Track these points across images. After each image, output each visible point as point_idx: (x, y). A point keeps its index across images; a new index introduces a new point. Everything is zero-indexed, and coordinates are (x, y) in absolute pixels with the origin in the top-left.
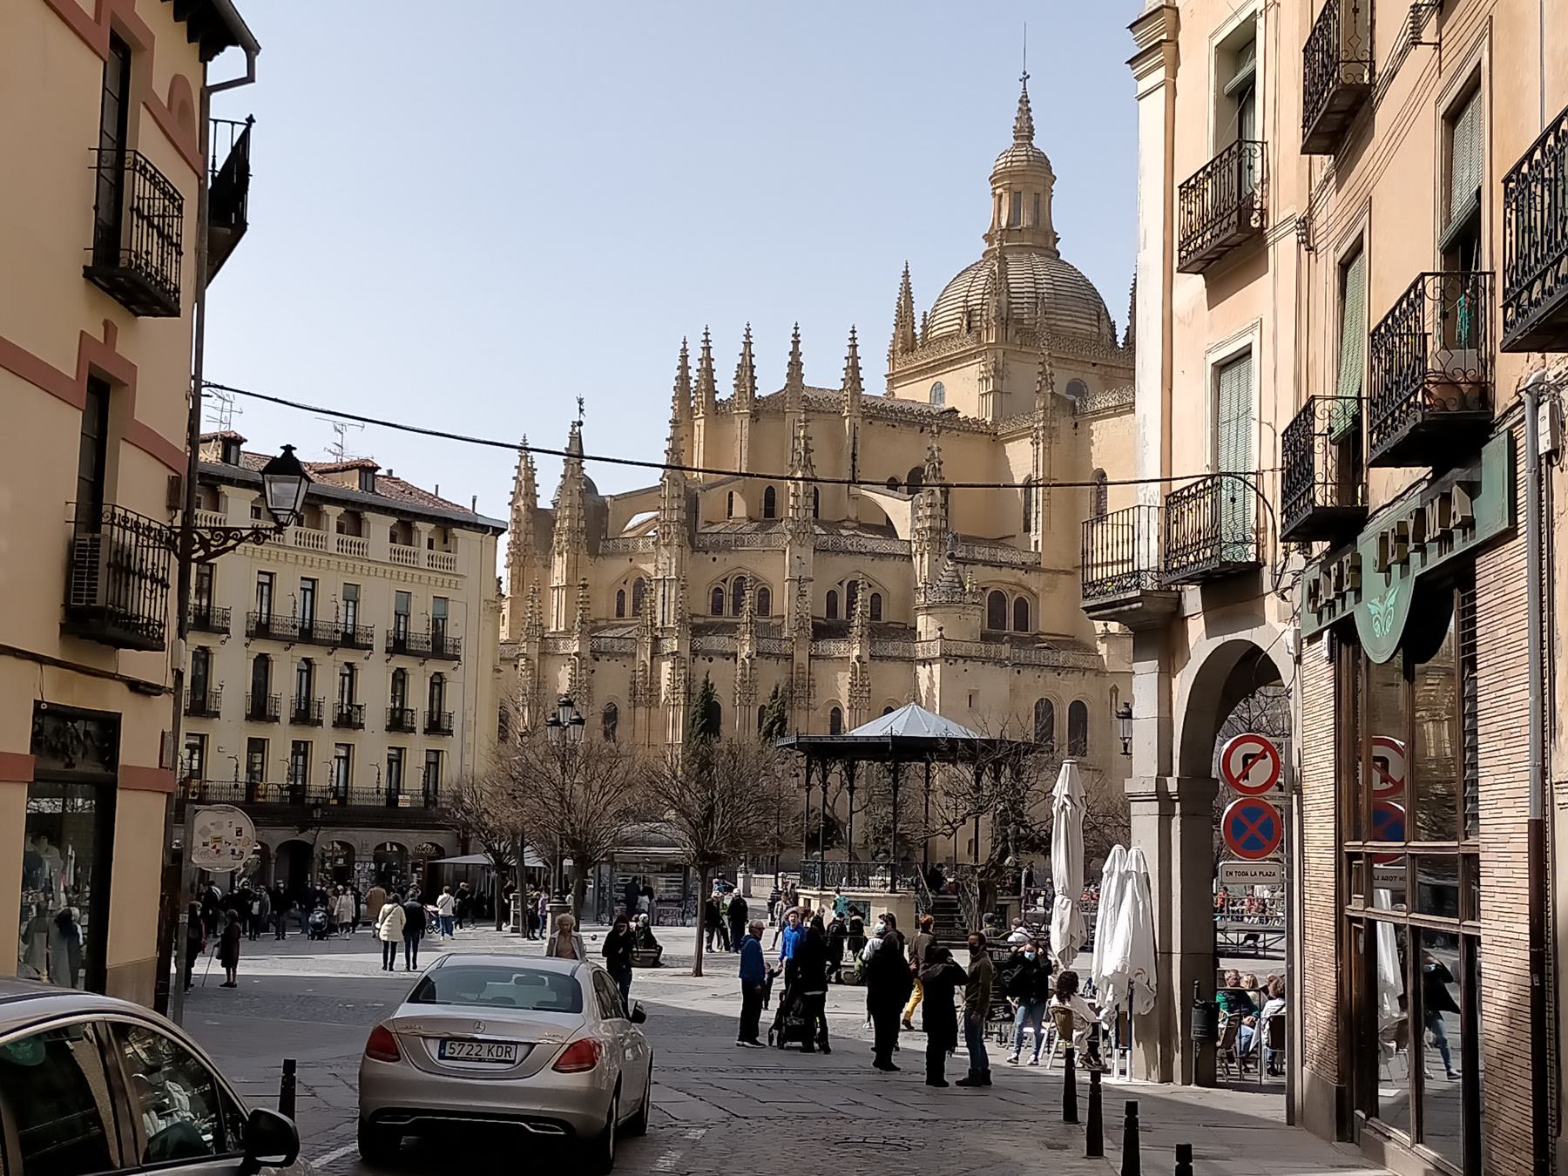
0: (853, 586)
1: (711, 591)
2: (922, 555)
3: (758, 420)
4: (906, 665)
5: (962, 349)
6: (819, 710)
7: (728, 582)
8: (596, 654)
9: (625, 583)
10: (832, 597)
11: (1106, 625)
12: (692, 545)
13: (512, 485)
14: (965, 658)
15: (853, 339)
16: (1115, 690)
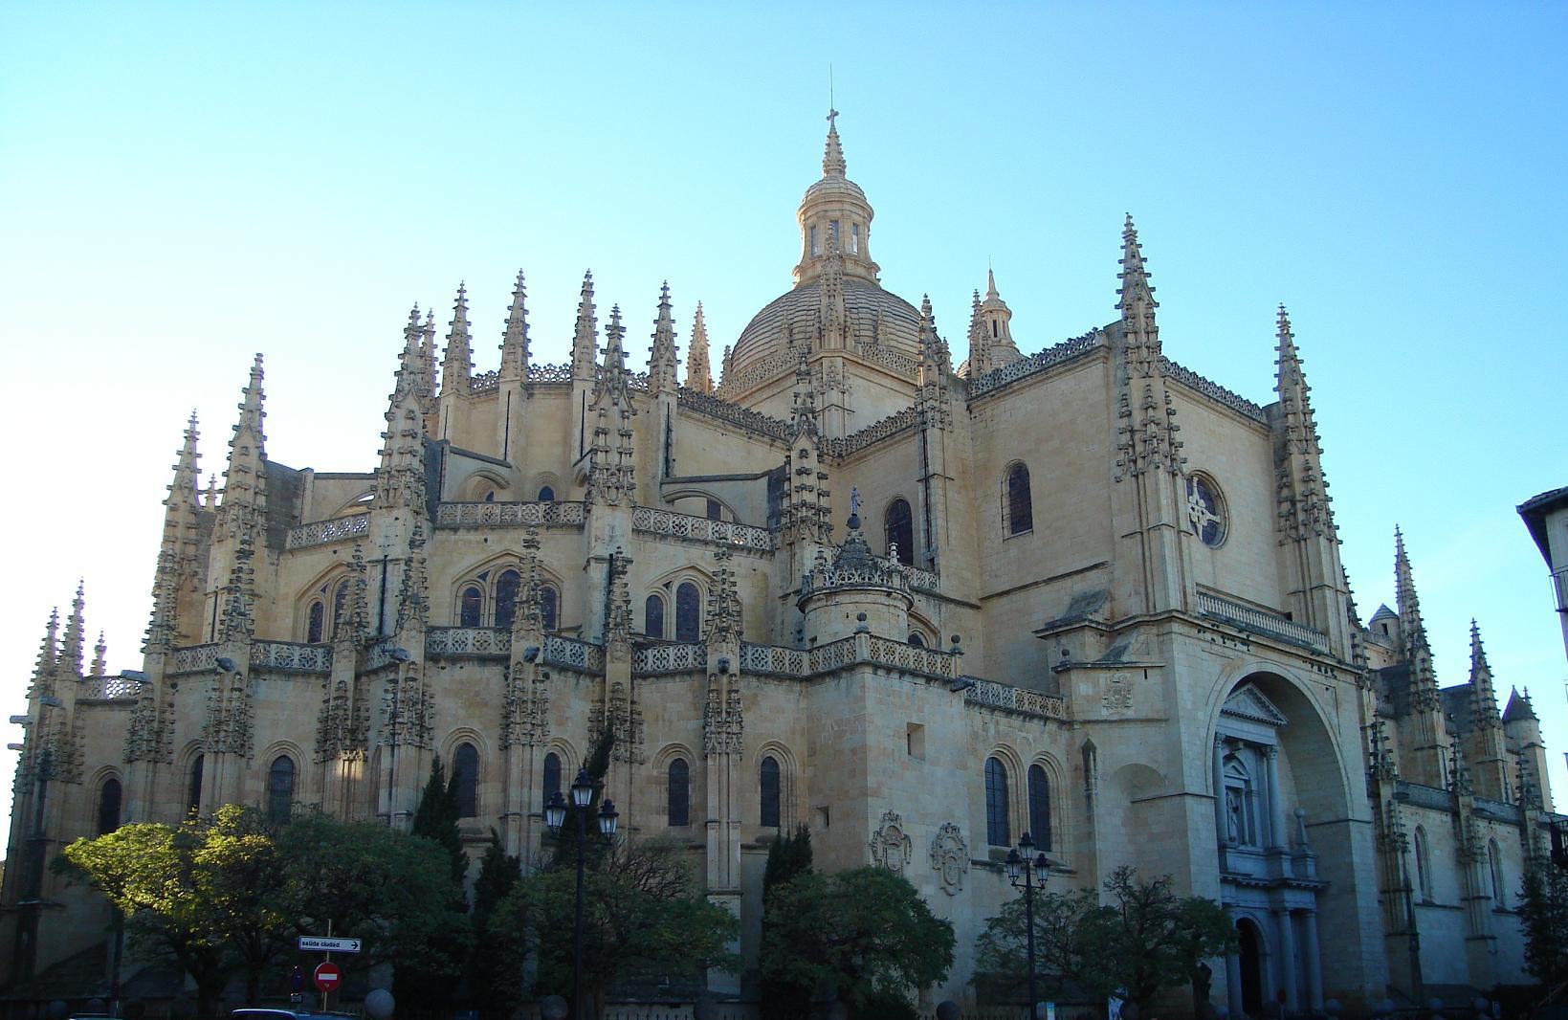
0: (688, 595)
1: (461, 594)
2: (791, 544)
3: (531, 395)
4: (797, 687)
5: (788, 365)
6: (649, 765)
7: (489, 578)
8: (256, 671)
9: (324, 590)
10: (654, 604)
11: (1065, 653)
12: (433, 519)
13: (170, 477)
14: (902, 672)
15: (664, 297)
16: (1088, 749)
